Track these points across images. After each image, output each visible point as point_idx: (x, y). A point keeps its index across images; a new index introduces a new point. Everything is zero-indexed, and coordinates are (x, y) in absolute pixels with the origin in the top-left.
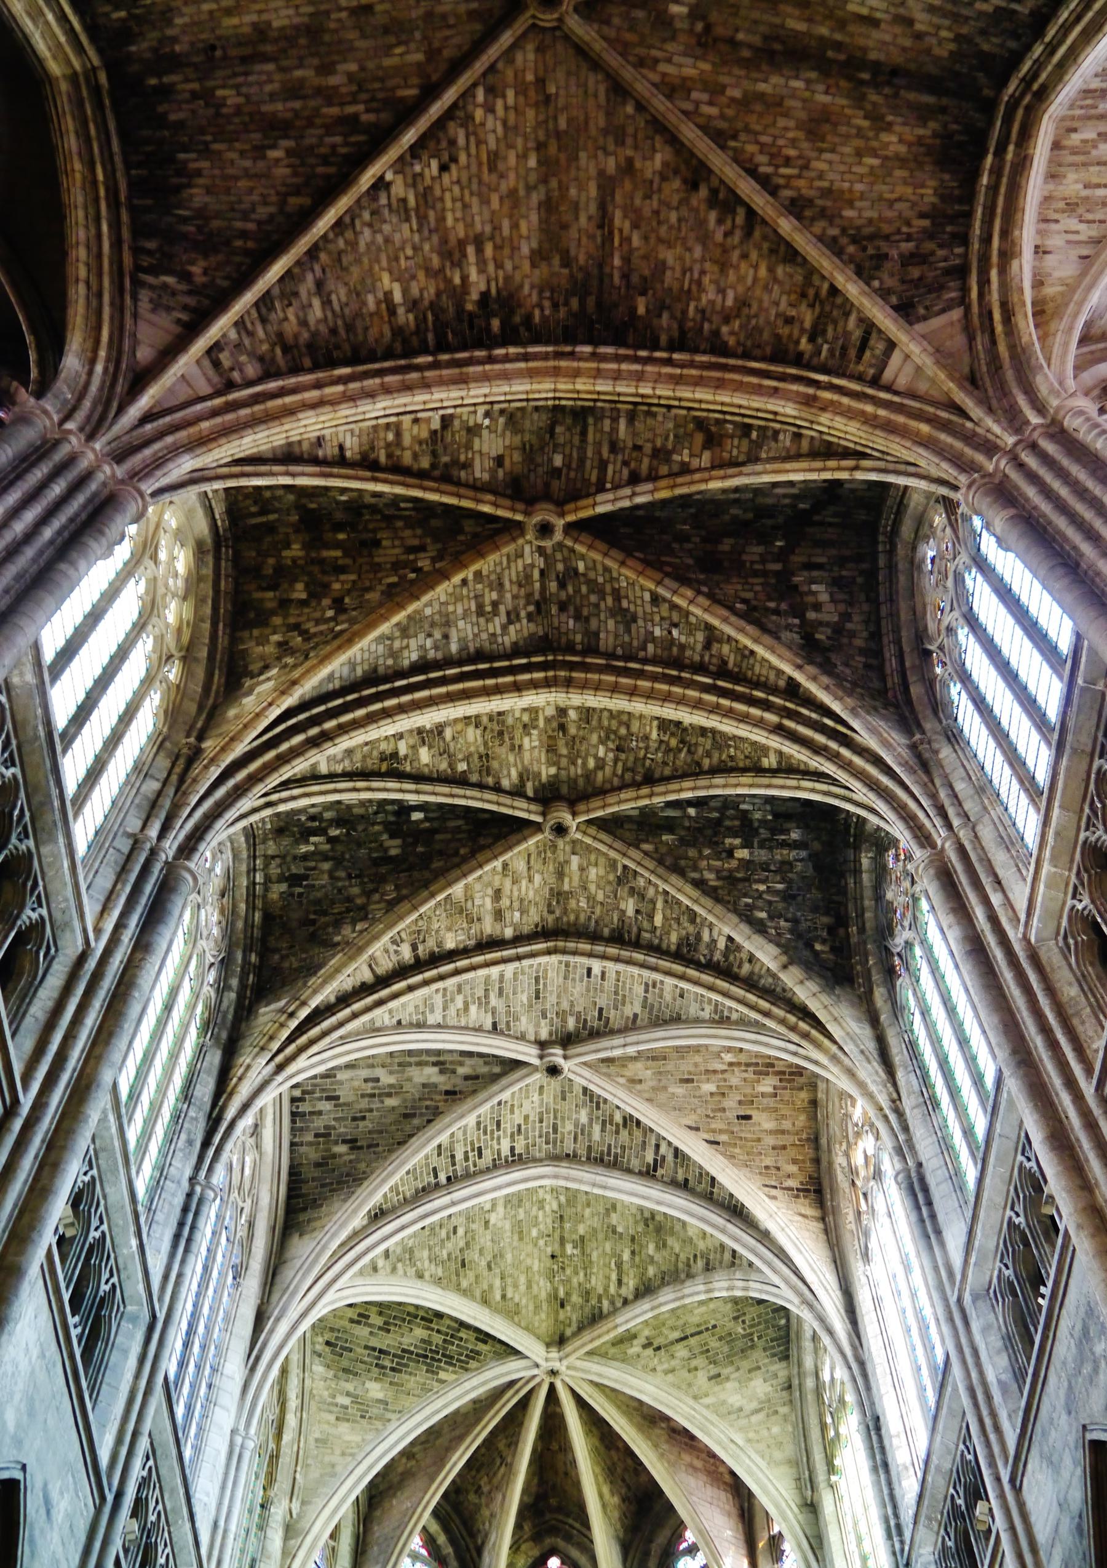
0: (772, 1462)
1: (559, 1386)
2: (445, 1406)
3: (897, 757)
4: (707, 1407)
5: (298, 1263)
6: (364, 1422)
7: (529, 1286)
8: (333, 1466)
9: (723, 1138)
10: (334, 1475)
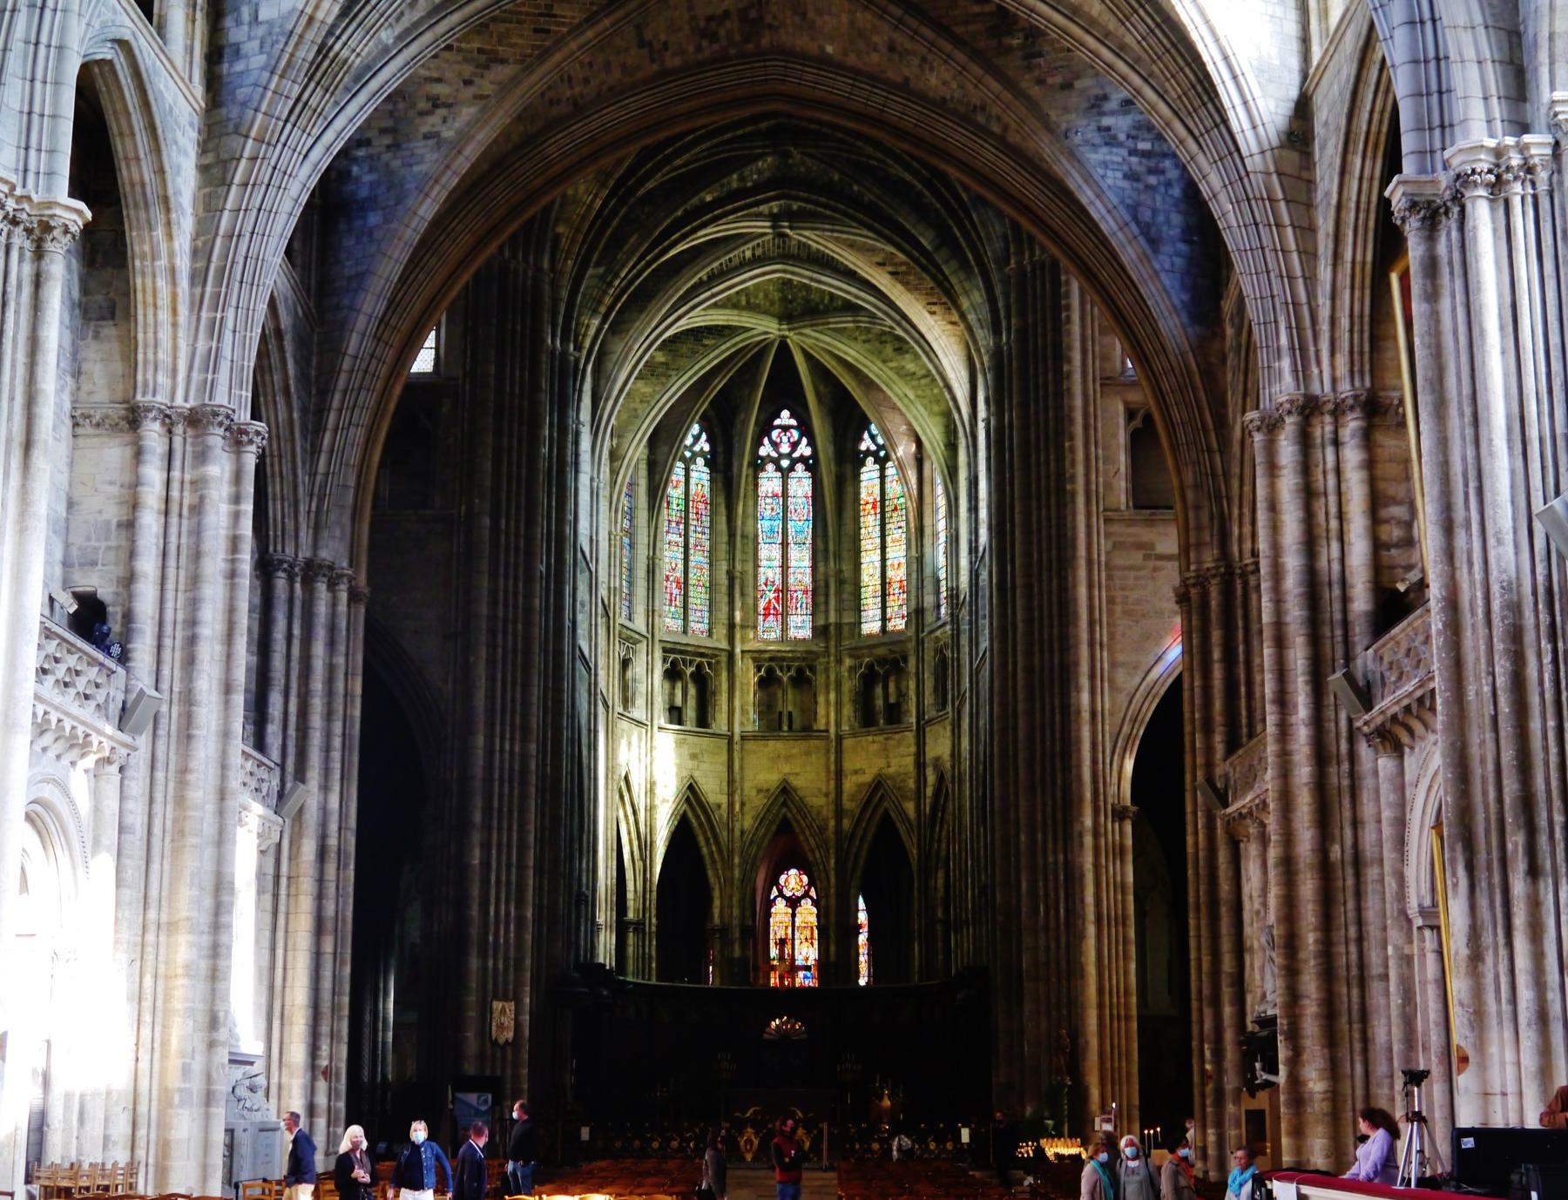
0: (931, 413)
1: (789, 341)
2: (708, 363)
3: (994, 252)
4: (891, 369)
5: (615, 357)
6: (654, 378)
7: (766, 296)
8: (636, 410)
9: (903, 268)
10: (637, 417)
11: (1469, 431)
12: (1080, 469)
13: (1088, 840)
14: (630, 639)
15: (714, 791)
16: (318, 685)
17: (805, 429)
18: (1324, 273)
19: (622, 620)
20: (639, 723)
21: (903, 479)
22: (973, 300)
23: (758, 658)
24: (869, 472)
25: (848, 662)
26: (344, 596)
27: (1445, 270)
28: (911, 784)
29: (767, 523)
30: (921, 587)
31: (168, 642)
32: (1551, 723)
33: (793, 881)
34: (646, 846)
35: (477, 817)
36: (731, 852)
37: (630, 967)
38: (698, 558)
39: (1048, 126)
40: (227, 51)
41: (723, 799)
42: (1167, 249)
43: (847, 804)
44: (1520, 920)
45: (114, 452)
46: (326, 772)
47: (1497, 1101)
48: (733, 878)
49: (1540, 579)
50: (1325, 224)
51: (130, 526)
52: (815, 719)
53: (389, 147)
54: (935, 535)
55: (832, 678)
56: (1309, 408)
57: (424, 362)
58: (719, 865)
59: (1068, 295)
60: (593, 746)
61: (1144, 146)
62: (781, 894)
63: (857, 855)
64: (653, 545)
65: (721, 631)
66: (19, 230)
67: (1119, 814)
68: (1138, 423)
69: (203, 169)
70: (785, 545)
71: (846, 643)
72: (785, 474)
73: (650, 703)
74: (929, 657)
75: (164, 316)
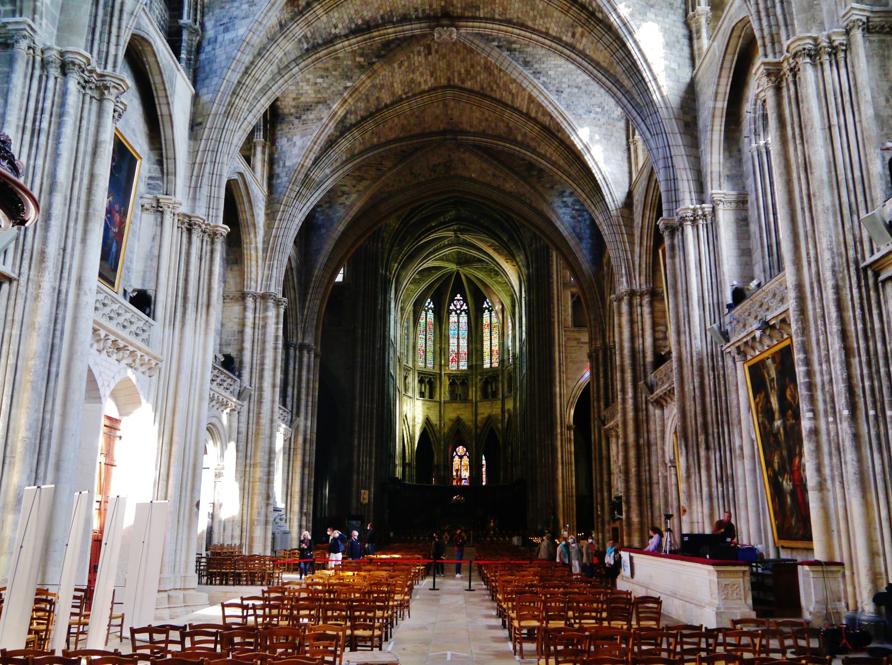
11: (685, 302)
12: (556, 314)
13: (559, 437)
14: (407, 370)
15: (434, 420)
16: (304, 385)
17: (465, 300)
18: (637, 249)
19: (404, 363)
20: (410, 397)
21: (498, 317)
22: (521, 258)
23: (449, 376)
24: (486, 315)
26: (313, 355)
27: (677, 249)
28: (500, 418)
29: (452, 332)
30: (503, 352)
31: (254, 371)
32: (713, 399)
33: (461, 450)
34: (412, 438)
35: (356, 428)
37: (407, 478)
38: (430, 343)
39: (546, 201)
40: (275, 177)
41: (438, 423)
42: (584, 241)
43: (479, 424)
44: (703, 464)
45: (236, 308)
46: (306, 414)
47: (696, 525)
49: (709, 351)
50: (637, 233)
51: (242, 332)
53: (328, 208)
54: (508, 335)
56: (632, 294)
57: (339, 278)
59: (552, 256)
60: (395, 405)
61: (577, 207)
64: (415, 338)
65: (437, 367)
66: (206, 235)
67: (569, 428)
68: (575, 298)
69: (267, 215)
70: (458, 338)
71: (479, 371)
72: (458, 315)
73: (414, 391)
74: (506, 375)
75: (254, 263)
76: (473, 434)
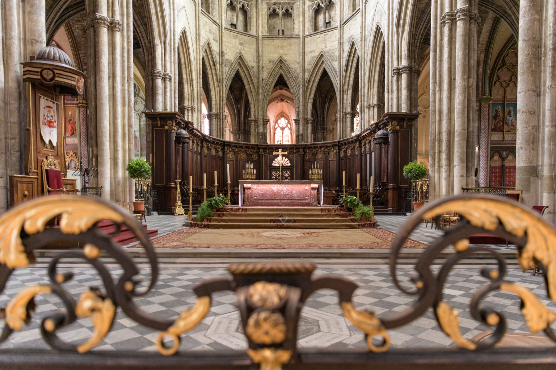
15: (250, 59)
25: (308, 3)
28: (337, 53)
36: (258, 87)
41: (255, 65)
43: (307, 66)
48: (259, 98)
52: (294, 31)
55: (301, 10)
58: (254, 93)
62: (279, 126)
63: (311, 89)
76: (300, 80)
